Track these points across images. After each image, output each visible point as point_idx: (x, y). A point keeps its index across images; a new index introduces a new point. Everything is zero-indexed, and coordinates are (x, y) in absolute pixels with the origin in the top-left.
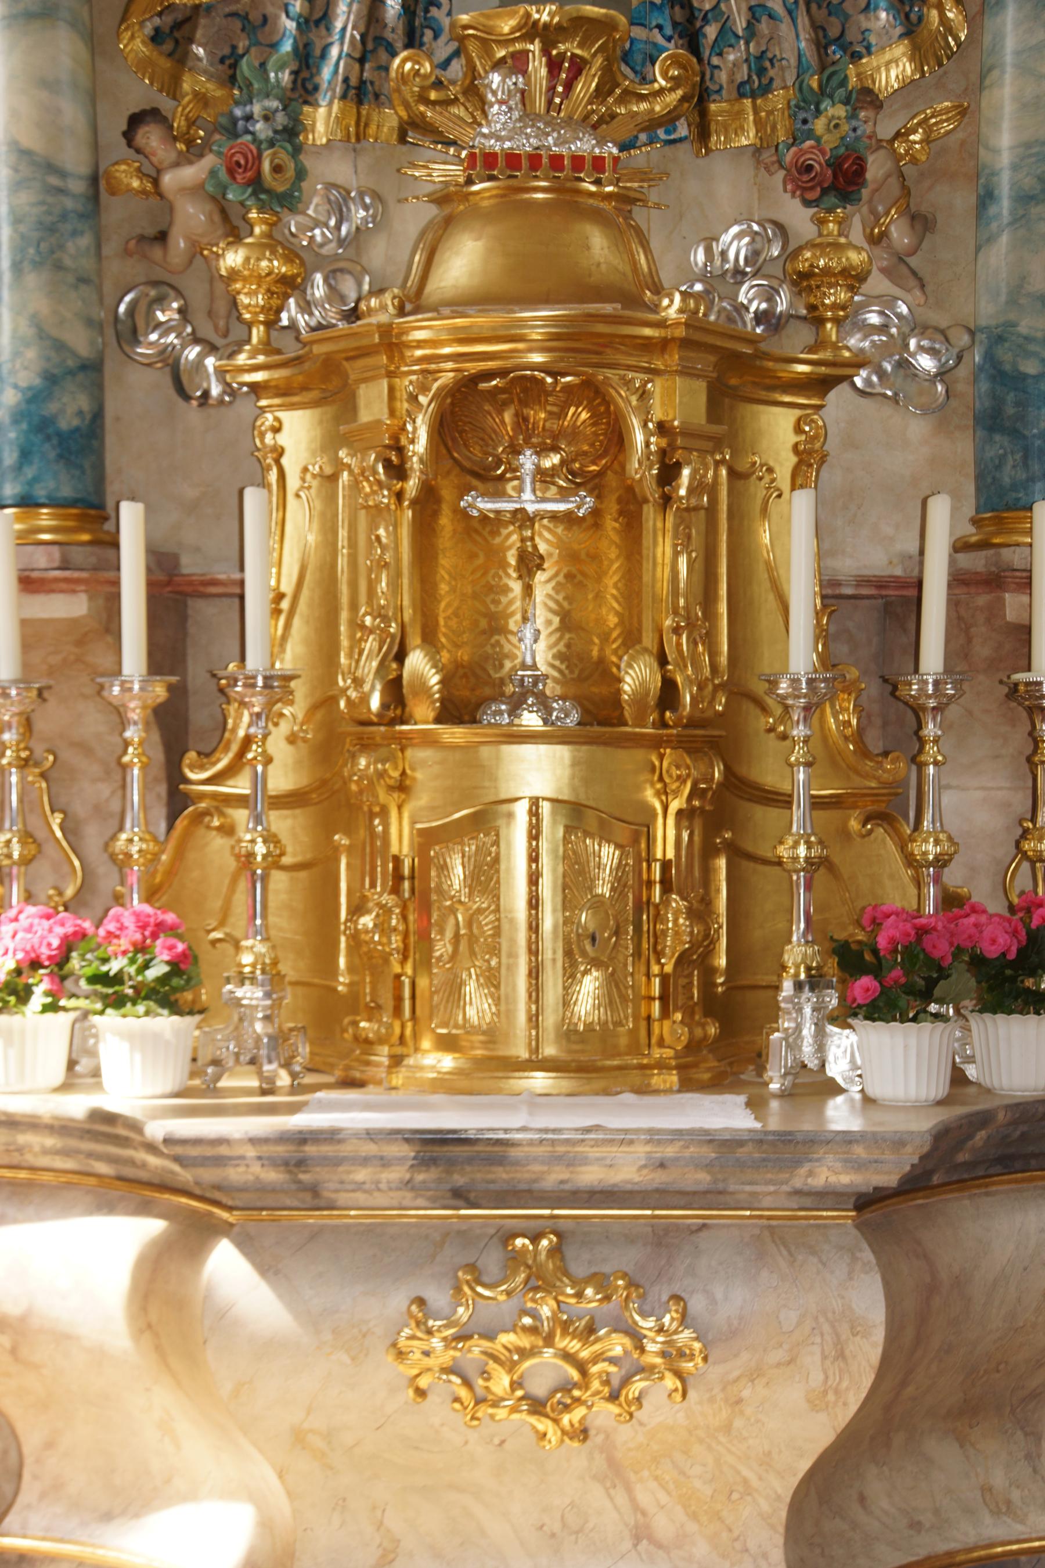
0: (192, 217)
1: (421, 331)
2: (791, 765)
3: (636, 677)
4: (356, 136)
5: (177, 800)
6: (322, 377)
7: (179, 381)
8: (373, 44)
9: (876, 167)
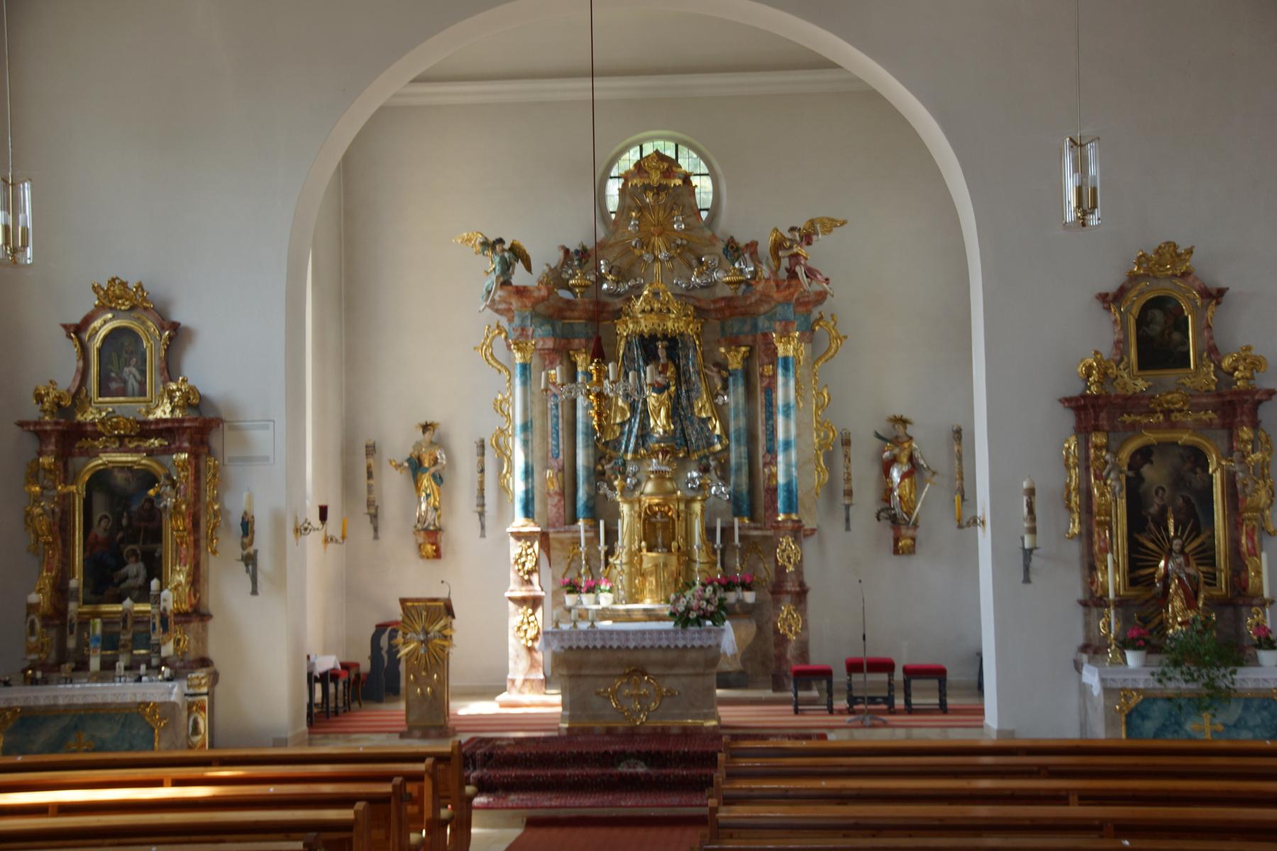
0: (608, 473)
1: (643, 498)
2: (699, 556)
3: (674, 544)
4: (634, 459)
5: (607, 564)
6: (631, 503)
7: (605, 496)
8: (637, 444)
9: (713, 463)
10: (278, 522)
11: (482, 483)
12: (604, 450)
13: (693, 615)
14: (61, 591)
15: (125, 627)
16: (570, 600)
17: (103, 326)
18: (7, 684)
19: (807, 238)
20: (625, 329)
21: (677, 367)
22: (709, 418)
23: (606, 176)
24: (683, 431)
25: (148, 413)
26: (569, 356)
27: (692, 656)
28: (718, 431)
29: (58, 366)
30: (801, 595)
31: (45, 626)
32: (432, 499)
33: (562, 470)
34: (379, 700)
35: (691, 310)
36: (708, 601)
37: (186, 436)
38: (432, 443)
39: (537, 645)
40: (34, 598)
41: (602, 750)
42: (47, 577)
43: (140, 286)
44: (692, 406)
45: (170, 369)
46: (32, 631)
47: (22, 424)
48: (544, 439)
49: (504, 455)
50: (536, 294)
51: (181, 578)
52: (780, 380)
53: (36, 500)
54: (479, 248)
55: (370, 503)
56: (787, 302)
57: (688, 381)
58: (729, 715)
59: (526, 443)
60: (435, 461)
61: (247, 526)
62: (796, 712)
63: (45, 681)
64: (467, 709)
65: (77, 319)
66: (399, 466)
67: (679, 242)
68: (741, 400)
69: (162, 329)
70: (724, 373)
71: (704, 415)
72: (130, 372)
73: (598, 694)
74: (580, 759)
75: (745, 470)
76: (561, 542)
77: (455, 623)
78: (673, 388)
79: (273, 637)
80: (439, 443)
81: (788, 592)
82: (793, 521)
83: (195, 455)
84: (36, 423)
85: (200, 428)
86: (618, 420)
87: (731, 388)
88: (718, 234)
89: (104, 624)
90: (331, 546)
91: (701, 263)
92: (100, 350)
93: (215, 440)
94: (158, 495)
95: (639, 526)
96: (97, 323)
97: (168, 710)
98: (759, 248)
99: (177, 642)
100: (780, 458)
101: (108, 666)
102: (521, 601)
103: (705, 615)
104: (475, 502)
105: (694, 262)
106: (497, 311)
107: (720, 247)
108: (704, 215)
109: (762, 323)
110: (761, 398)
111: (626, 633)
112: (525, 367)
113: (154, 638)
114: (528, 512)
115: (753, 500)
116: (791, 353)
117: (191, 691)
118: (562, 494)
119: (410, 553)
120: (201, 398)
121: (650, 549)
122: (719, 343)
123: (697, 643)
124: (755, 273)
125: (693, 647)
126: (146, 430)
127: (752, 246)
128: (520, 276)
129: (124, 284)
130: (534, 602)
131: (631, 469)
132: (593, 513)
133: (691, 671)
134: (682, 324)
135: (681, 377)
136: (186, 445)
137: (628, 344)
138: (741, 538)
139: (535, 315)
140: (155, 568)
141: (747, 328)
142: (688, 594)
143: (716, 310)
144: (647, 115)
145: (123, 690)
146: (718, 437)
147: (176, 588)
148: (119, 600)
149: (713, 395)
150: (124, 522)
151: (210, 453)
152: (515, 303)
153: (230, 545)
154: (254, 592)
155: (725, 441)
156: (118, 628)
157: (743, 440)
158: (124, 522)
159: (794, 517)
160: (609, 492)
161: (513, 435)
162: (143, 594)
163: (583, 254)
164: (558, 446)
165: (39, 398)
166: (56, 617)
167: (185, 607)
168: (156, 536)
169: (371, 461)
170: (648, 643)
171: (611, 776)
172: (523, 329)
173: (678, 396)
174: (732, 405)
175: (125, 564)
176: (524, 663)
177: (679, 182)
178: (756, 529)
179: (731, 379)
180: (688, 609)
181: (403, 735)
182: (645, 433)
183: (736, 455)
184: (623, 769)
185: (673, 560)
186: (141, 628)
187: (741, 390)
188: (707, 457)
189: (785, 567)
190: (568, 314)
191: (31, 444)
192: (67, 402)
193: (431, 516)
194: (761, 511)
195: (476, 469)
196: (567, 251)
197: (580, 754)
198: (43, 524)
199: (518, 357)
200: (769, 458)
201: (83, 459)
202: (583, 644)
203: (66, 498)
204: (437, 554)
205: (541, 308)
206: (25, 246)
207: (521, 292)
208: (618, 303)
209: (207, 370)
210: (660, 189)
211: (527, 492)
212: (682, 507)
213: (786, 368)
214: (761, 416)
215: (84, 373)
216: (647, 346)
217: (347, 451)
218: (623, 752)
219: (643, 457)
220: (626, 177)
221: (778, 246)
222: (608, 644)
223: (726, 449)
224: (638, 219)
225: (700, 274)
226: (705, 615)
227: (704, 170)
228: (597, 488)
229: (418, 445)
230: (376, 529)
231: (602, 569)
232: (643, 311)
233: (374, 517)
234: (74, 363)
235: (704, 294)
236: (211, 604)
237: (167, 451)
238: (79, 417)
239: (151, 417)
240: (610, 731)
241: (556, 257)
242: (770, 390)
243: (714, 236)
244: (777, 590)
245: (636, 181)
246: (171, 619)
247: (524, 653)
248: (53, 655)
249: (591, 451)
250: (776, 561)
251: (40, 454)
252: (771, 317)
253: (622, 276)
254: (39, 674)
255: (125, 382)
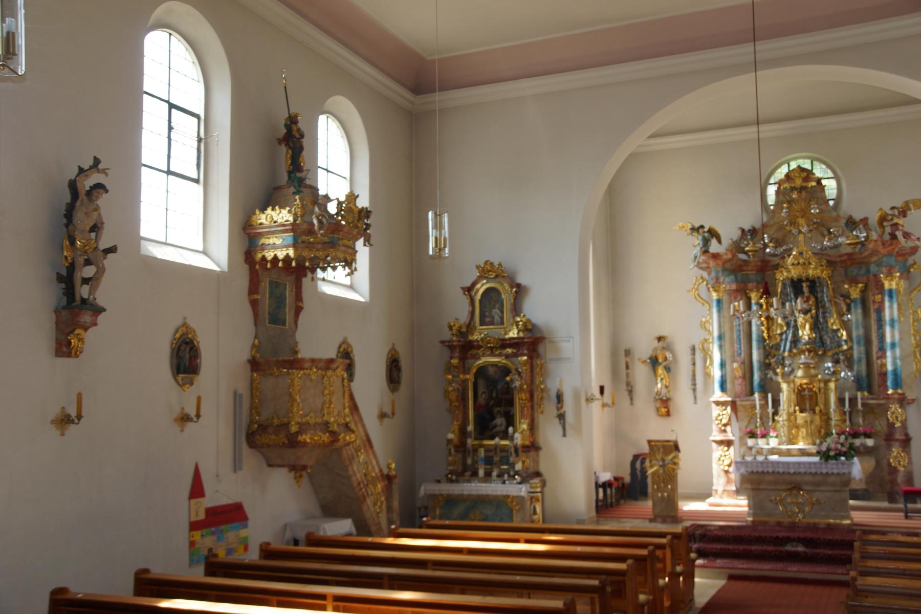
0: (773, 364)
2: (835, 416)
3: (817, 409)
4: (789, 356)
5: (774, 420)
6: (788, 383)
7: (771, 378)
8: (791, 347)
9: (842, 358)
10: (576, 395)
11: (694, 371)
12: (770, 352)
13: (832, 453)
14: (463, 433)
15: (496, 453)
16: (750, 442)
17: (482, 287)
18: (439, 481)
19: (903, 213)
20: (781, 276)
21: (816, 298)
22: (838, 330)
23: (767, 183)
24: (821, 338)
25: (506, 334)
26: (746, 294)
27: (831, 479)
28: (844, 337)
29: (459, 310)
30: (906, 442)
31: (456, 451)
32: (664, 381)
33: (743, 363)
34: (636, 499)
35: (824, 262)
36: (842, 445)
37: (525, 347)
38: (663, 348)
39: (731, 469)
40: (451, 436)
41: (775, 535)
42: (456, 425)
43: (500, 265)
44: (826, 322)
45: (516, 309)
46: (450, 454)
47: (442, 342)
48: (732, 344)
49: (707, 354)
50: (725, 257)
51: (525, 426)
52: (887, 304)
53: (450, 383)
54: (689, 231)
55: (628, 384)
56: (890, 254)
57: (824, 307)
58: (858, 517)
59: (721, 347)
60: (666, 359)
61: (559, 398)
62: (907, 517)
63: (457, 481)
64: (688, 506)
65: (468, 284)
66: (644, 362)
67: (815, 220)
68: (860, 317)
69: (512, 287)
70: (848, 301)
71: (835, 327)
72: (496, 312)
73: (771, 501)
74: (760, 540)
75: (864, 362)
76: (744, 407)
77: (681, 455)
78: (814, 311)
79: (577, 461)
80: (668, 348)
81: (897, 440)
82: (899, 394)
83: (531, 357)
84: (450, 341)
85: (533, 342)
86: (779, 332)
87: (853, 310)
88: (841, 214)
89: (486, 451)
90: (606, 409)
91: (830, 233)
92: (480, 301)
93: (541, 349)
94: (512, 380)
95: (794, 397)
96: (478, 286)
97: (520, 499)
98: (870, 222)
99: (524, 462)
100: (889, 353)
101: (488, 474)
102: (720, 443)
103: (840, 454)
104: (690, 383)
105: (826, 233)
106: (701, 268)
107: (843, 222)
108: (831, 203)
109: (873, 268)
110: (873, 316)
111: (788, 464)
112: (719, 301)
113: (511, 459)
114: (723, 388)
115: (870, 380)
116: (894, 287)
117: (532, 490)
118: (744, 377)
119: (652, 413)
120: (534, 325)
121: (802, 411)
122: (844, 283)
123: (835, 471)
124: (867, 238)
125: (833, 473)
126: (505, 344)
127: (865, 221)
128: (714, 247)
129: (492, 264)
130: (728, 443)
131: (787, 362)
132: (764, 390)
133: (831, 488)
134: (818, 271)
135: (819, 304)
136: (526, 352)
137: (784, 285)
138: (863, 405)
139: (724, 270)
140: (510, 421)
141: (863, 272)
142: (829, 440)
143: (841, 262)
144: (791, 145)
145: (495, 488)
146: (846, 341)
147: (522, 433)
148: (492, 438)
149: (841, 315)
150: (494, 395)
151: (538, 356)
152: (712, 263)
153: (550, 408)
154: (564, 435)
155: (850, 344)
156: (491, 454)
157: (862, 342)
158: (494, 395)
159: (900, 391)
160: (774, 377)
161: (713, 343)
162: (505, 435)
163: (754, 232)
164: (740, 348)
165: (450, 328)
166: (461, 447)
167: (527, 443)
168: (511, 403)
169: (628, 359)
170: (802, 470)
171: (781, 552)
172: (717, 278)
173: (817, 316)
174: (854, 321)
175: (494, 418)
176: (723, 480)
177: (814, 184)
178: (873, 399)
179: (853, 305)
180: (829, 450)
181: (651, 521)
182: (796, 340)
183: (858, 352)
184: (789, 548)
185: (817, 419)
186: (504, 454)
187: (859, 311)
188: (837, 354)
189: (894, 424)
190: (745, 268)
191: (447, 352)
192: (464, 330)
193: (664, 391)
194: (876, 388)
195: (690, 363)
196: (743, 231)
197: (760, 537)
198: (453, 396)
199: (715, 295)
200: (880, 354)
201: (471, 361)
202: (760, 470)
203: (465, 382)
204: (668, 414)
205: (728, 266)
206: (445, 247)
207: (715, 256)
208: (776, 260)
209: (537, 310)
210: (802, 189)
211: (722, 377)
212: (822, 385)
213: (891, 297)
214: (874, 327)
215: (472, 313)
216: (796, 286)
217: (614, 354)
218: (788, 538)
219: (795, 355)
220: (779, 183)
221: (883, 219)
222: (777, 470)
223: (851, 348)
224: (788, 208)
225: (830, 240)
226: (840, 454)
227: (830, 174)
228: (766, 374)
229: (655, 349)
230: (631, 399)
231: (770, 423)
232: (793, 264)
233: (630, 392)
234: (467, 308)
235: (833, 252)
236: (541, 441)
237: (515, 355)
238: (471, 338)
239: (507, 337)
240: (779, 524)
241: (736, 235)
242: (880, 311)
243: (838, 216)
244: (889, 438)
245: (786, 185)
246: (520, 449)
247: (722, 474)
248: (460, 469)
249: (762, 351)
250: (888, 419)
251: (451, 358)
252: (879, 264)
253: (778, 243)
254: (454, 477)
255: (493, 318)
